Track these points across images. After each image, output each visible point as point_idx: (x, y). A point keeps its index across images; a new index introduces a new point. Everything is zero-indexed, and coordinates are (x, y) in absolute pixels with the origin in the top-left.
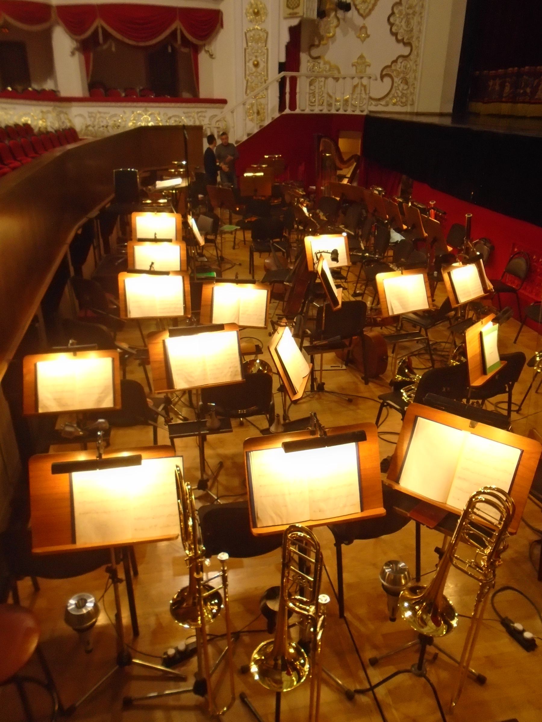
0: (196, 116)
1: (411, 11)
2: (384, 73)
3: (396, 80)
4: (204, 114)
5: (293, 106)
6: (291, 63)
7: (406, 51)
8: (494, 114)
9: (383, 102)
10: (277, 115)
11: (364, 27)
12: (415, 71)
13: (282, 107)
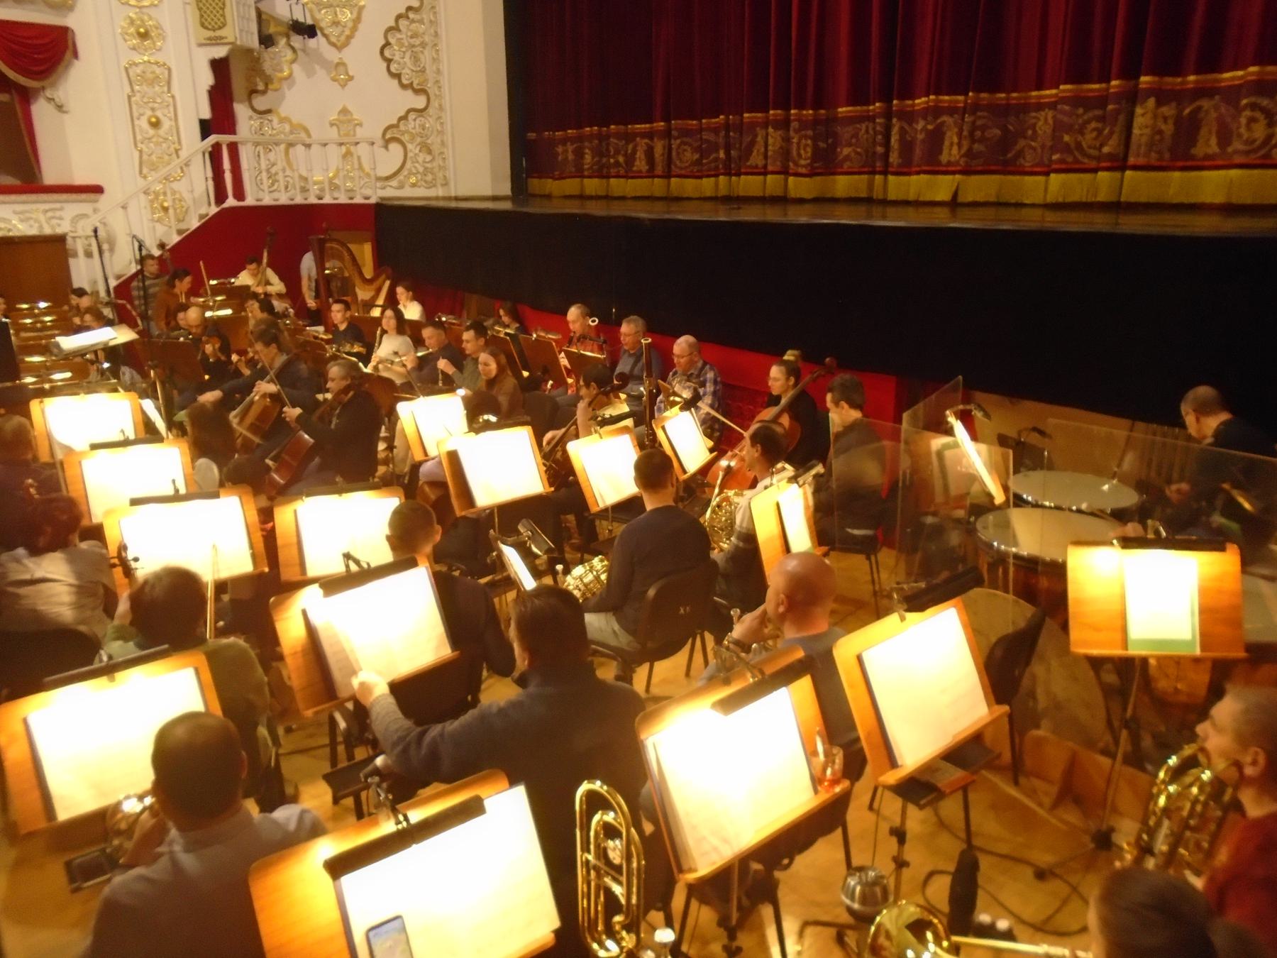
0: (42, 218)
1: (417, 41)
2: (388, 136)
3: (410, 146)
4: (58, 214)
5: (239, 194)
6: (219, 120)
7: (420, 102)
8: (559, 193)
9: (394, 183)
10: (214, 210)
11: (341, 64)
12: (441, 133)
13: (220, 196)
